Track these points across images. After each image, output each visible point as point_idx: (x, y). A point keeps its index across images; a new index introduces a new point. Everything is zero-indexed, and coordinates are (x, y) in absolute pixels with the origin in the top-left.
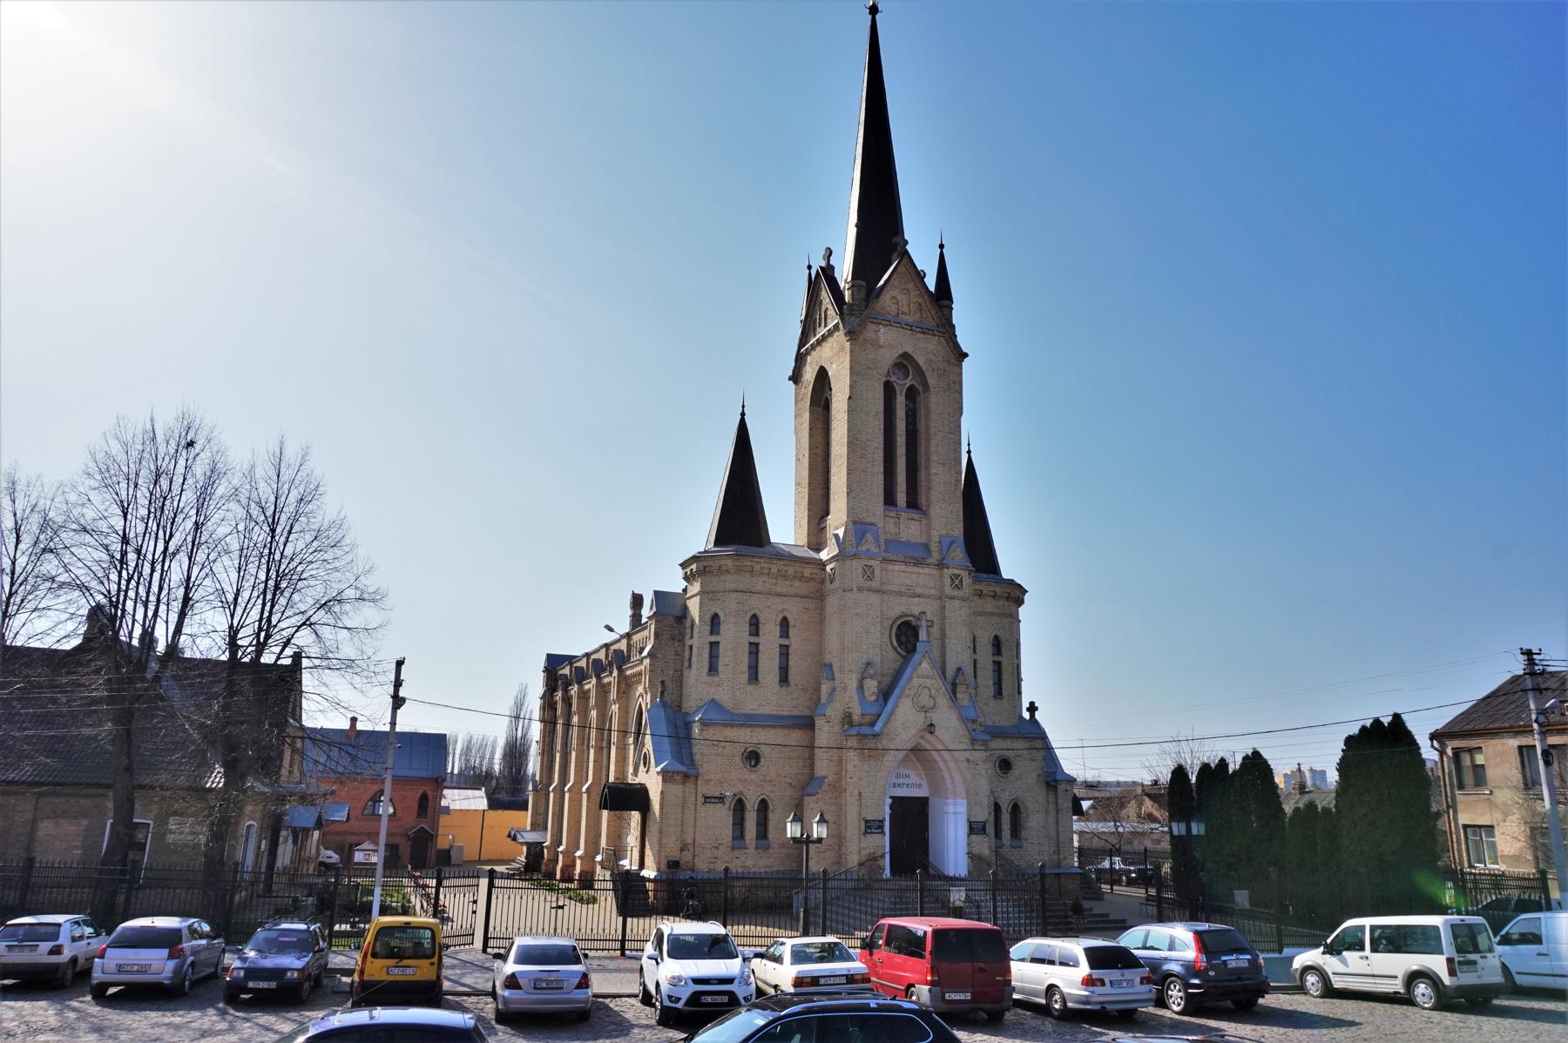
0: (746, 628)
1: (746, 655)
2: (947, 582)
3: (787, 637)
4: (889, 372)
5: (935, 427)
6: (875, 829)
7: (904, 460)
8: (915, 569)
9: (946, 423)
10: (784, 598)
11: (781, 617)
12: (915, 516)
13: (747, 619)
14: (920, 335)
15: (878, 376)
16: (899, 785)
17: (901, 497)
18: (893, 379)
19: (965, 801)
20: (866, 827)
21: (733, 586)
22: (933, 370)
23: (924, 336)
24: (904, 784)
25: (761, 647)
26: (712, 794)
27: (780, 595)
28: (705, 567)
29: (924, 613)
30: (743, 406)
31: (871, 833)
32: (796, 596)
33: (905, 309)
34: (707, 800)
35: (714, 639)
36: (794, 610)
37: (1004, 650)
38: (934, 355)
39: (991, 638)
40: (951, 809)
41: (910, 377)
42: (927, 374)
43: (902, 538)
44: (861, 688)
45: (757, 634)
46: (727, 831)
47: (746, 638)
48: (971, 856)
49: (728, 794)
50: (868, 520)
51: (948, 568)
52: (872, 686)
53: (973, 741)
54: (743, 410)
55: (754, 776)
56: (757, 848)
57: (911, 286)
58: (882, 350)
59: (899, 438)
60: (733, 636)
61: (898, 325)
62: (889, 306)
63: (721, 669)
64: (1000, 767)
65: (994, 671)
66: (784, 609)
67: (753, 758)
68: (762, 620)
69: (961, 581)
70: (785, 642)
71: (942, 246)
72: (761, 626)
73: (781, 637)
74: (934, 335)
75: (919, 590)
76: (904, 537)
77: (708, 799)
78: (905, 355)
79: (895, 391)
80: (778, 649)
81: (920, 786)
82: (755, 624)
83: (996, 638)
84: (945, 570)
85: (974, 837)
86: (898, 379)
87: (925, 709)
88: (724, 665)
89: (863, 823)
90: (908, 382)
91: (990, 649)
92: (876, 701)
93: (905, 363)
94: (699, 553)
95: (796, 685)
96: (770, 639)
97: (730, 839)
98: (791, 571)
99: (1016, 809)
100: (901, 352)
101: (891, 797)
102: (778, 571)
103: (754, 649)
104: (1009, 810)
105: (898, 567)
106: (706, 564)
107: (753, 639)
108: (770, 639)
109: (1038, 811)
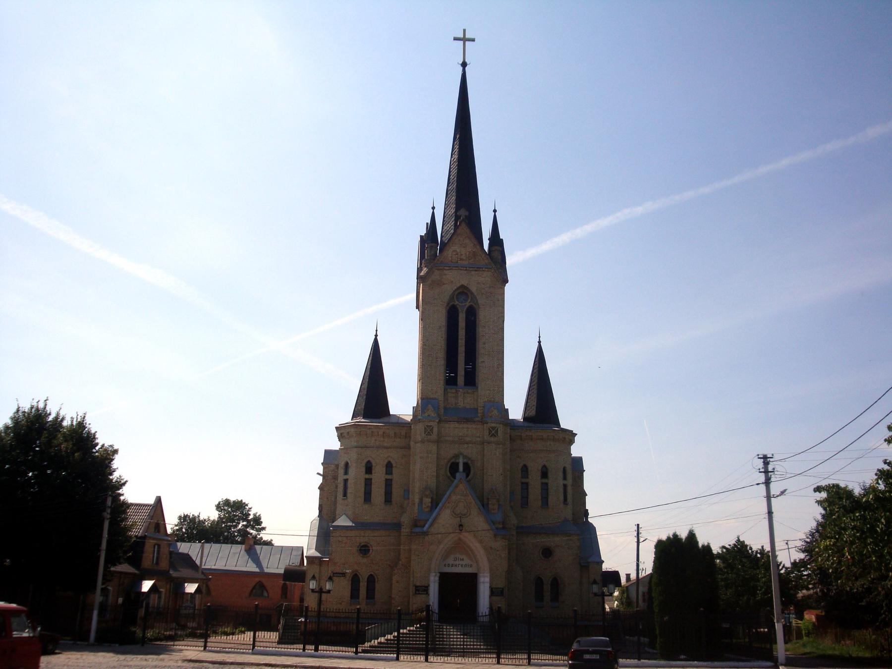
0: (363, 469)
3: (391, 474)
4: (453, 297)
5: (483, 331)
6: (422, 591)
8: (465, 426)
9: (491, 327)
10: (389, 449)
11: (386, 461)
12: (470, 391)
13: (364, 465)
14: (473, 273)
15: (441, 303)
16: (456, 566)
17: (461, 380)
18: (457, 303)
19: (488, 575)
20: (416, 590)
22: (482, 294)
23: (476, 272)
24: (459, 564)
25: (373, 481)
26: (338, 571)
27: (386, 448)
28: (341, 434)
31: (419, 594)
33: (463, 257)
34: (336, 575)
35: (345, 477)
36: (394, 456)
37: (550, 475)
38: (484, 284)
39: (540, 468)
41: (469, 300)
42: (478, 297)
43: (460, 406)
44: (421, 500)
46: (347, 592)
47: (363, 476)
48: (491, 608)
49: (347, 571)
50: (432, 396)
51: (487, 423)
52: (427, 501)
53: (495, 536)
54: (376, 333)
55: (365, 560)
57: (467, 241)
58: (445, 286)
59: (460, 341)
60: (356, 475)
61: (456, 268)
62: (451, 257)
63: (348, 495)
64: (542, 553)
65: (542, 490)
66: (389, 456)
69: (497, 431)
70: (389, 477)
71: (495, 211)
72: (373, 468)
74: (484, 271)
75: (468, 439)
76: (461, 405)
77: (335, 574)
78: (462, 286)
79: (458, 310)
80: (384, 482)
81: (471, 566)
83: (544, 467)
84: (485, 425)
85: (494, 598)
86: (462, 303)
87: (459, 516)
88: (350, 493)
89: (414, 587)
90: (468, 304)
91: (539, 474)
93: (463, 292)
94: (340, 425)
95: (396, 504)
97: (349, 599)
99: (556, 583)
100: (458, 285)
101: (440, 573)
102: (384, 433)
103: (368, 483)
104: (550, 583)
105: (453, 425)
106: (342, 431)
107: (367, 476)
108: (379, 476)
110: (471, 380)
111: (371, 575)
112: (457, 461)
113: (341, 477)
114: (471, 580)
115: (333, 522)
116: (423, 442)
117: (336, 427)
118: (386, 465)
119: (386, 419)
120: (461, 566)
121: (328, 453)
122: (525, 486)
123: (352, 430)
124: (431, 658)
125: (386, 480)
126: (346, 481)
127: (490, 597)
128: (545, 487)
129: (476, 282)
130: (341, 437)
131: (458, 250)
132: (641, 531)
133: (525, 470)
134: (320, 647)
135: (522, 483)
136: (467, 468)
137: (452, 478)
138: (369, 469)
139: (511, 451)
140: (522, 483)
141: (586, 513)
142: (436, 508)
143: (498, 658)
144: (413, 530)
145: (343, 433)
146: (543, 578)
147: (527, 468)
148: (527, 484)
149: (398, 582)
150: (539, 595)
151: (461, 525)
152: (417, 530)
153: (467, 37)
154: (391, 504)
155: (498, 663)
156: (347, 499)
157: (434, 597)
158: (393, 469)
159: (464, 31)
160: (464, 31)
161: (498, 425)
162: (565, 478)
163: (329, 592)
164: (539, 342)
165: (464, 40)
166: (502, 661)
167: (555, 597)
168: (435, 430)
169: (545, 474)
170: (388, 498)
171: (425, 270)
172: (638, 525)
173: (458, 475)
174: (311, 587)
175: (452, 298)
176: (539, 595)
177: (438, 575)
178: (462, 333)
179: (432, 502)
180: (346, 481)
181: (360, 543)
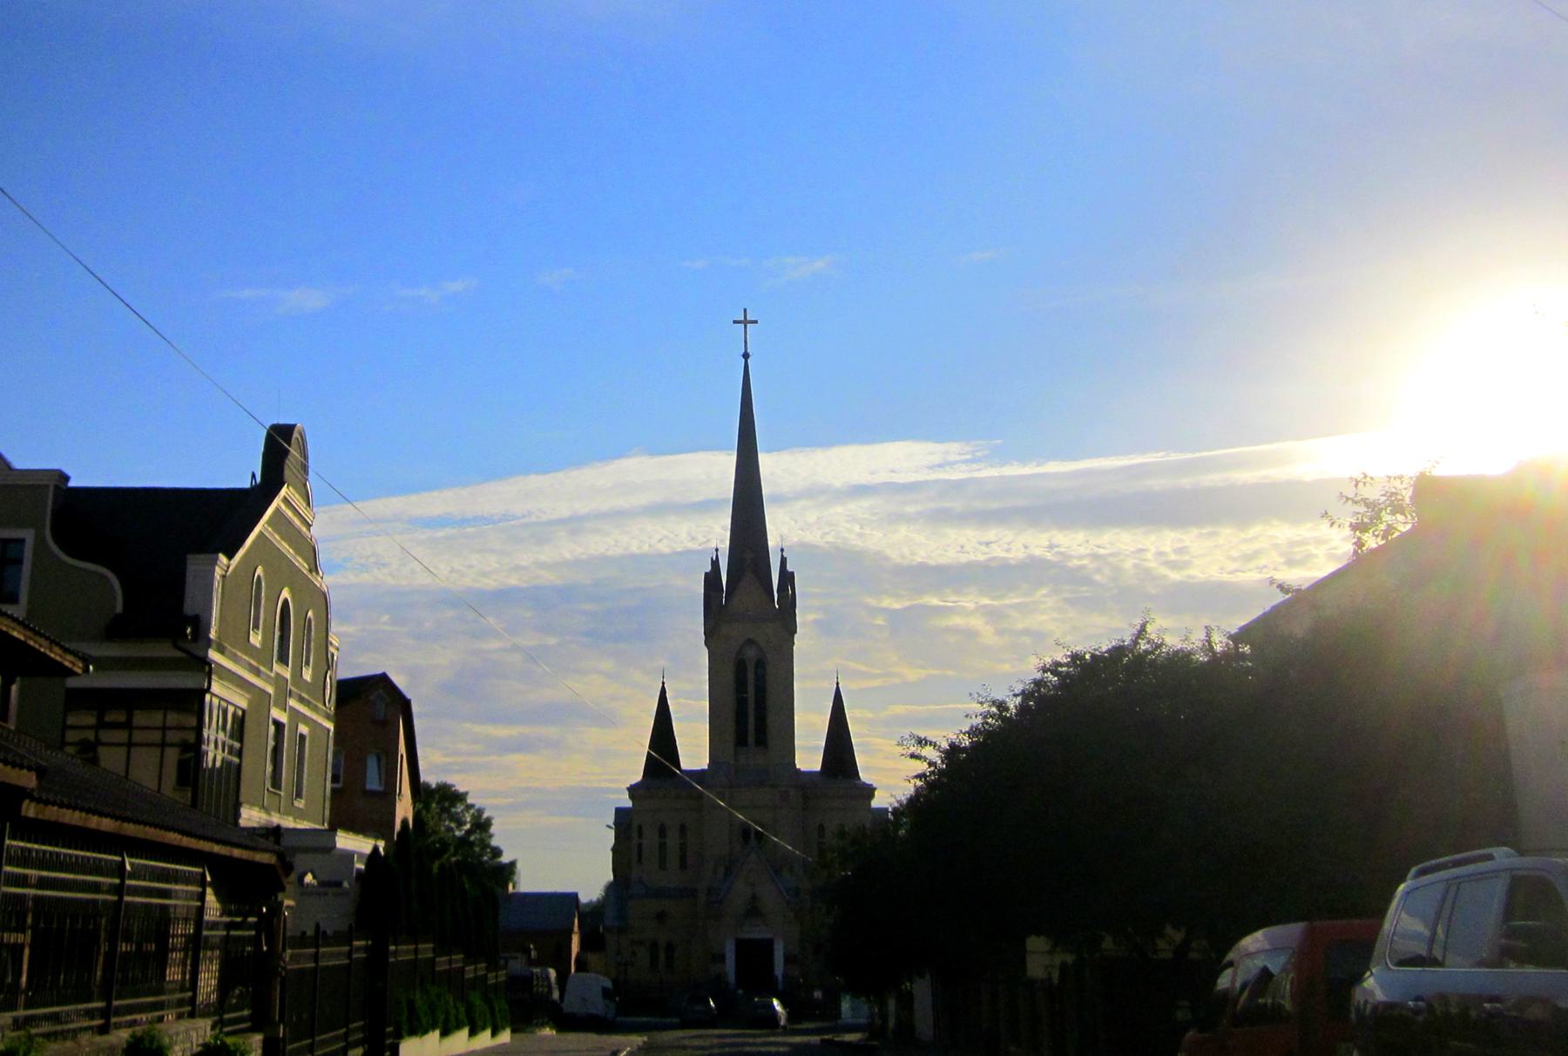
40: (776, 947)
45: (665, 836)
52: (721, 870)
60: (650, 839)
71: (782, 550)
78: (749, 640)
82: (662, 831)
96: (673, 841)
103: (662, 846)
108: (673, 841)
110: (762, 741)
113: (635, 841)
114: (768, 945)
117: (628, 789)
120: (756, 932)
126: (640, 846)
130: (632, 797)
133: (821, 828)
138: (662, 831)
159: (745, 310)
160: (745, 310)
165: (745, 322)
170: (683, 865)
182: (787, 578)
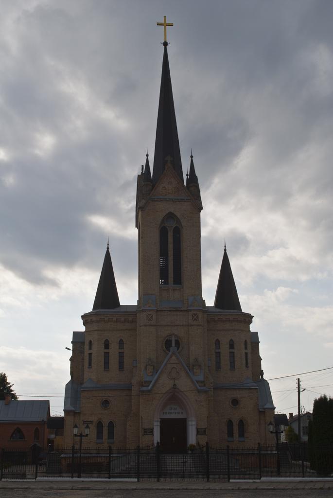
1: (103, 358)
2: (190, 317)
7: (172, 262)
8: (175, 313)
11: (119, 340)
13: (103, 342)
20: (144, 432)
21: (96, 328)
25: (110, 354)
28: (86, 320)
29: (173, 334)
30: (108, 245)
31: (147, 434)
32: (126, 330)
35: (90, 352)
40: (190, 423)
42: (181, 221)
44: (146, 368)
47: (103, 350)
52: (150, 368)
53: (199, 391)
56: (108, 443)
60: (97, 350)
63: (93, 365)
64: (232, 402)
65: (230, 357)
67: (106, 403)
68: (110, 342)
69: (198, 317)
71: (192, 157)
73: (119, 348)
74: (185, 201)
77: (84, 422)
81: (182, 413)
82: (107, 346)
83: (231, 340)
84: (189, 312)
85: (199, 436)
91: (228, 346)
92: (152, 375)
93: (171, 216)
94: (84, 314)
96: (114, 350)
98: (123, 319)
99: (241, 423)
100: (167, 212)
101: (161, 419)
102: (117, 319)
103: (107, 355)
106: (87, 319)
107: (106, 351)
108: (114, 350)
109: (254, 424)
110: (178, 280)
111: (111, 421)
112: (171, 339)
113: (87, 352)
115: (81, 384)
116: (145, 325)
118: (120, 342)
119: (117, 310)
120: (175, 414)
121: (75, 334)
122: (218, 355)
123: (94, 318)
124: (162, 480)
125: (120, 353)
126: (90, 354)
127: (196, 435)
128: (232, 355)
129: (179, 210)
131: (166, 187)
132: (300, 383)
133: (218, 343)
134: (82, 475)
135: (216, 353)
136: (178, 343)
137: (167, 351)
138: (107, 346)
139: (207, 330)
140: (216, 353)
141: (262, 373)
142: (157, 373)
143: (208, 478)
144: (142, 389)
145: (88, 320)
146: (233, 421)
147: (219, 342)
148: (219, 353)
149: (131, 426)
150: (230, 434)
151: (175, 385)
152: (144, 389)
153: (167, 22)
154: (123, 371)
155: (208, 481)
156: (91, 368)
157: (157, 437)
158: (124, 345)
159: (165, 17)
160: (165, 17)
161: (198, 312)
162: (246, 348)
163: (87, 435)
164: (225, 250)
165: (165, 25)
166: (210, 479)
167: (242, 434)
168: (154, 317)
169: (232, 346)
170: (121, 367)
171: (143, 202)
172: (299, 379)
173: (171, 349)
174: (75, 433)
175: (163, 221)
176: (230, 434)
177: (160, 420)
178: (171, 246)
179: (153, 369)
180: (90, 354)
181: (102, 399)
182: (193, 178)
